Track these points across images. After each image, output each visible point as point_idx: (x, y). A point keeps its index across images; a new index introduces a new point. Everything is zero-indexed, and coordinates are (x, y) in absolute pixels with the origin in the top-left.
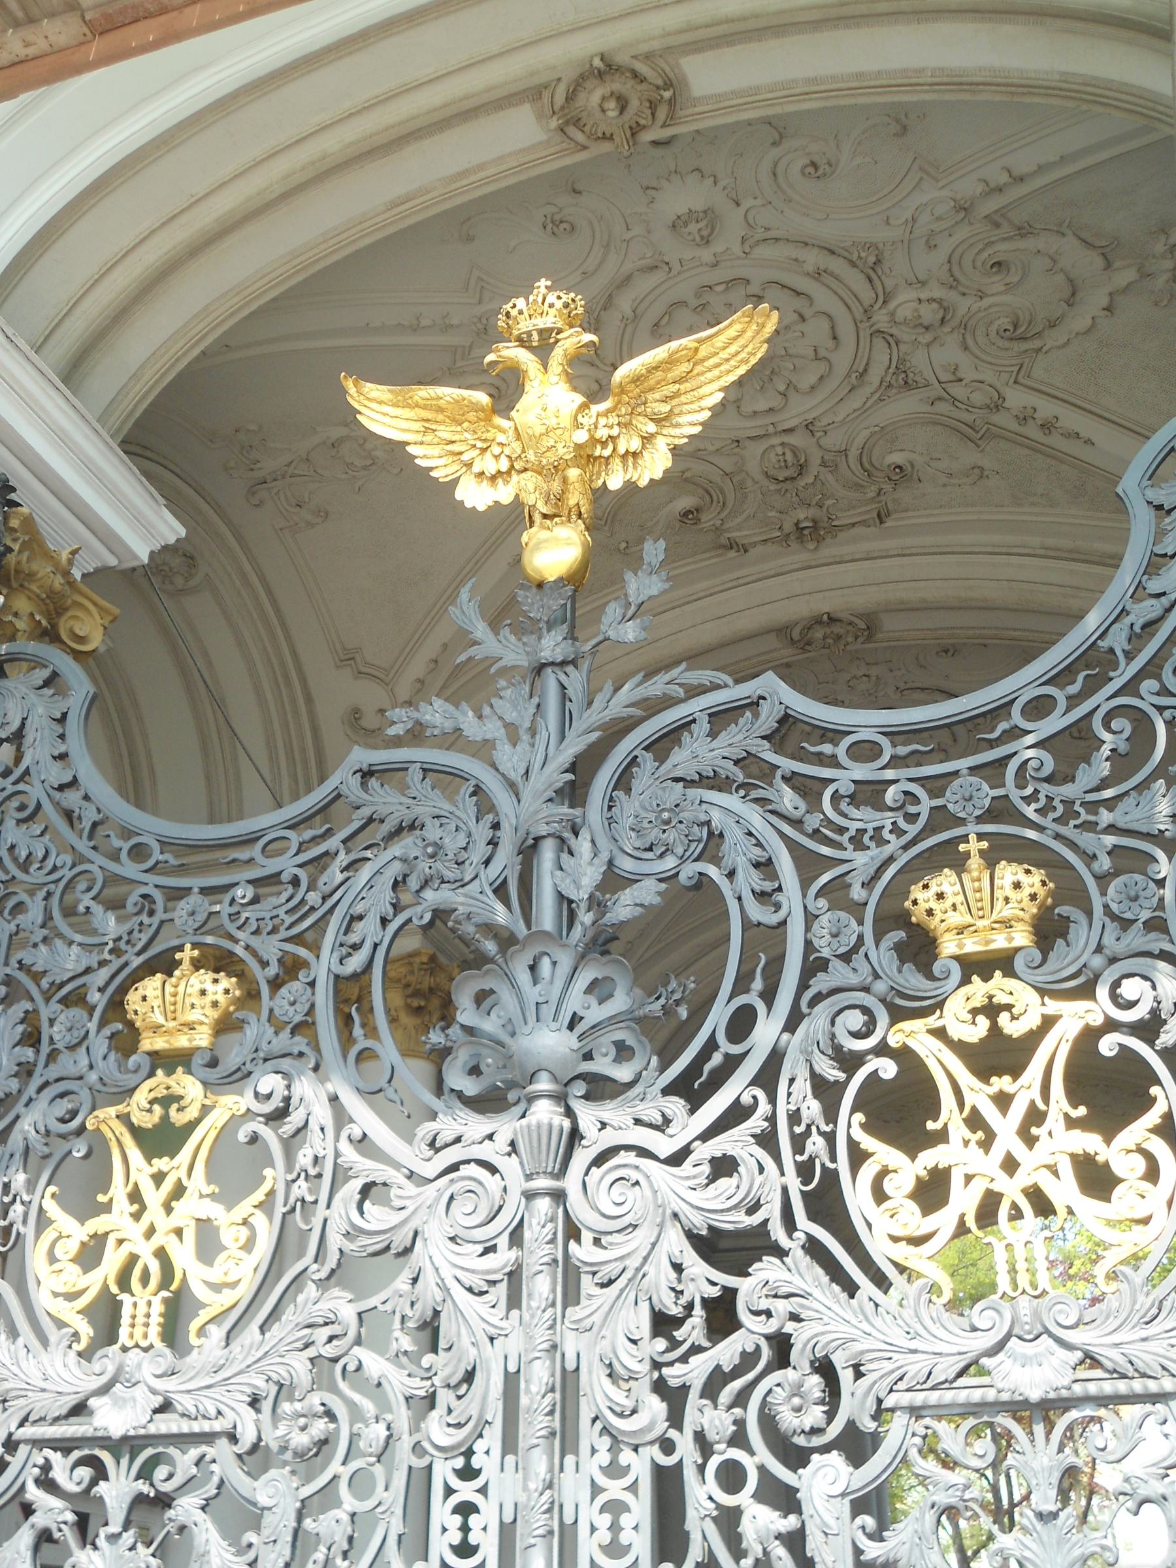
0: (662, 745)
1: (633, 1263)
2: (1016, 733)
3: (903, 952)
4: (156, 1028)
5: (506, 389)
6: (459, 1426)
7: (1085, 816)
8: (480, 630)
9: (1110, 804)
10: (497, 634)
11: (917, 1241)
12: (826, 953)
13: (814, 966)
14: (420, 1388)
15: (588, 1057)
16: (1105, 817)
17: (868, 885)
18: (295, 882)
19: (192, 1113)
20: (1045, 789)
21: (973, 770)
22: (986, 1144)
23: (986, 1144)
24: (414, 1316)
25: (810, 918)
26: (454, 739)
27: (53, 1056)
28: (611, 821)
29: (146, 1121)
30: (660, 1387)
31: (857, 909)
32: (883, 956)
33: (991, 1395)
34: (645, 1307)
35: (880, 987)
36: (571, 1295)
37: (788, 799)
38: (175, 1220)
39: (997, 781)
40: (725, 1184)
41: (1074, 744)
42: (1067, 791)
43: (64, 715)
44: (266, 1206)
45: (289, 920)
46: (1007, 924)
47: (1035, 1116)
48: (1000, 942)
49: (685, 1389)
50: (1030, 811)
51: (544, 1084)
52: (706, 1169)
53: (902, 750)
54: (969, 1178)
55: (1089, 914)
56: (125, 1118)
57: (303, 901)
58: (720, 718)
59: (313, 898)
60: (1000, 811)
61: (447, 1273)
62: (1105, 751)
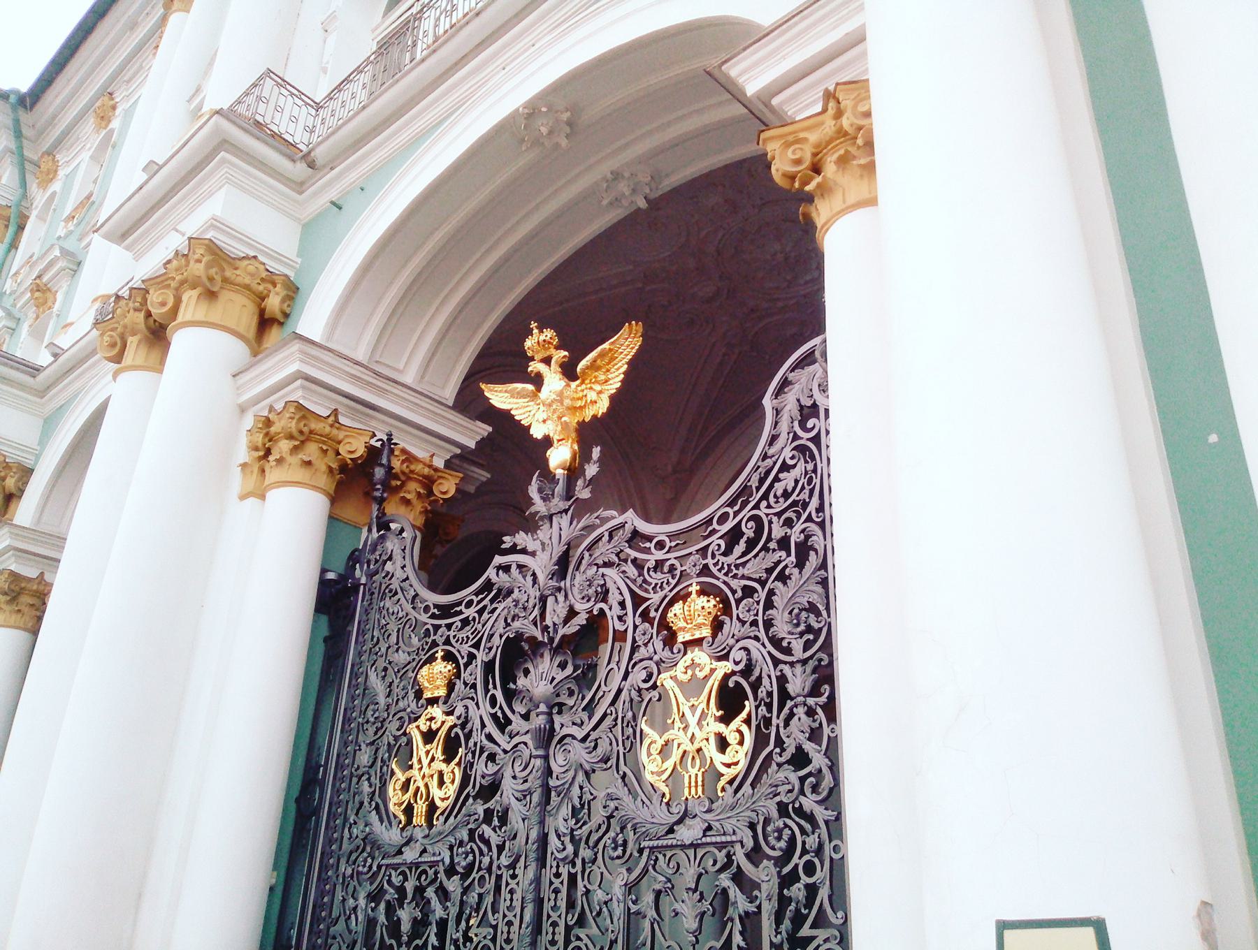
5: (538, 381)
7: (735, 571)
15: (558, 695)
16: (741, 572)
17: (656, 610)
18: (474, 619)
20: (722, 559)
25: (635, 627)
26: (524, 551)
32: (659, 644)
33: (675, 842)
35: (656, 658)
37: (632, 571)
42: (730, 559)
46: (699, 626)
47: (703, 716)
54: (679, 745)
56: (418, 727)
60: (705, 571)
62: (745, 538)
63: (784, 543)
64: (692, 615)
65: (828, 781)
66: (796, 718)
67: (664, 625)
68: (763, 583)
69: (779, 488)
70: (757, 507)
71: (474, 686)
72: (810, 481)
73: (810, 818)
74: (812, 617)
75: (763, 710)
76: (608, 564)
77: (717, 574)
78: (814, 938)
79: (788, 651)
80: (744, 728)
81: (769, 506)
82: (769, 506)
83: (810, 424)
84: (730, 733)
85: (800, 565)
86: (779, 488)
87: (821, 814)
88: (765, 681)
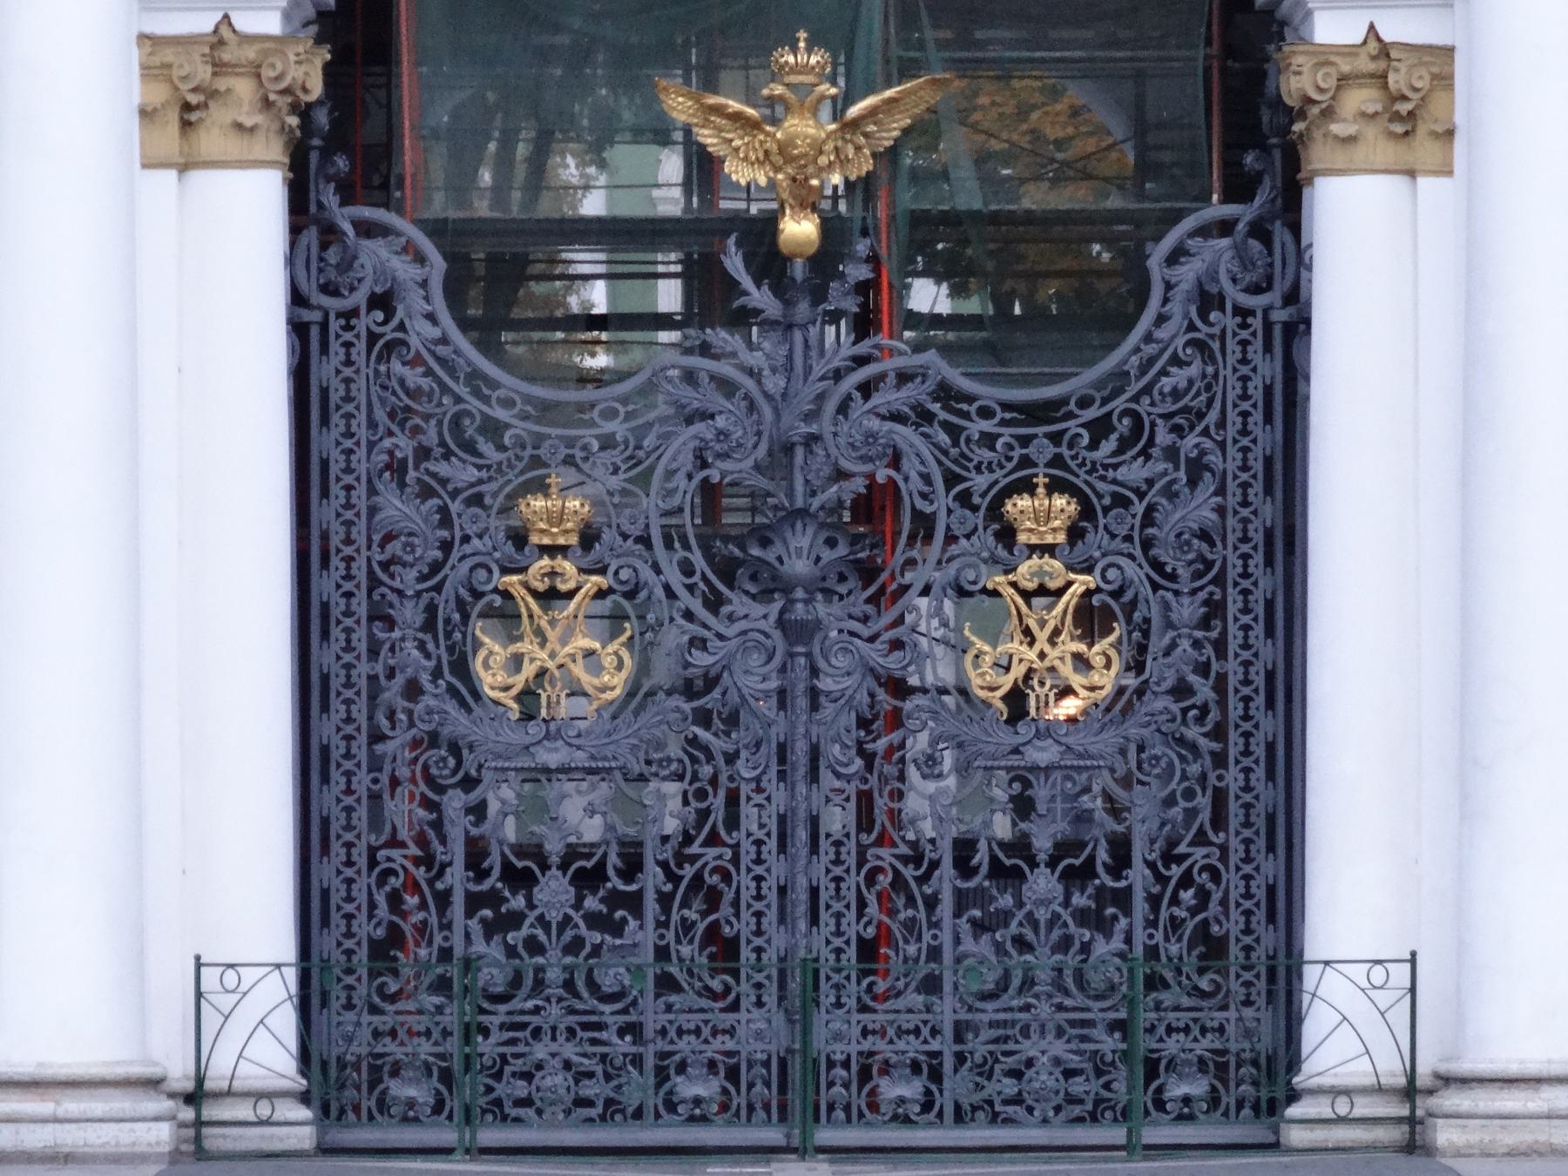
0: (866, 389)
1: (849, 692)
2: (1070, 416)
3: (998, 536)
4: (543, 531)
6: (755, 768)
8: (747, 282)
9: (1116, 467)
10: (759, 288)
11: (992, 689)
12: (957, 533)
13: (951, 539)
14: (730, 748)
16: (1111, 474)
17: (983, 495)
18: (626, 443)
19: (571, 585)
20: (1084, 453)
21: (1046, 435)
22: (1031, 644)
23: (1031, 644)
24: (726, 712)
25: (950, 511)
27: (466, 539)
28: (835, 434)
29: (541, 587)
30: (861, 752)
31: (975, 509)
33: (1023, 763)
34: (853, 714)
36: (815, 706)
37: (943, 438)
38: (568, 649)
39: (1057, 443)
40: (898, 654)
41: (1099, 429)
43: (425, 281)
44: (630, 643)
45: (623, 467)
47: (1056, 632)
48: (1049, 539)
49: (874, 754)
50: (1072, 464)
51: (800, 593)
52: (886, 646)
53: (1008, 416)
54: (1021, 661)
55: (1096, 527)
57: (631, 457)
58: (904, 378)
59: (641, 454)
60: (1057, 462)
61: (745, 691)
63: (1172, 454)
64: (1042, 514)
65: (1214, 715)
66: (1179, 649)
67: (995, 511)
68: (1141, 495)
69: (1166, 383)
70: (1135, 399)
71: (645, 541)
72: (1208, 387)
73: (1193, 747)
74: (1205, 546)
75: (1136, 635)
76: (897, 417)
77: (1076, 469)
78: (1188, 855)
79: (1173, 577)
80: (1112, 653)
81: (1153, 404)
82: (1153, 404)
83: (1213, 316)
84: (1095, 654)
85: (1193, 483)
86: (1166, 383)
87: (1205, 744)
88: (1141, 606)
